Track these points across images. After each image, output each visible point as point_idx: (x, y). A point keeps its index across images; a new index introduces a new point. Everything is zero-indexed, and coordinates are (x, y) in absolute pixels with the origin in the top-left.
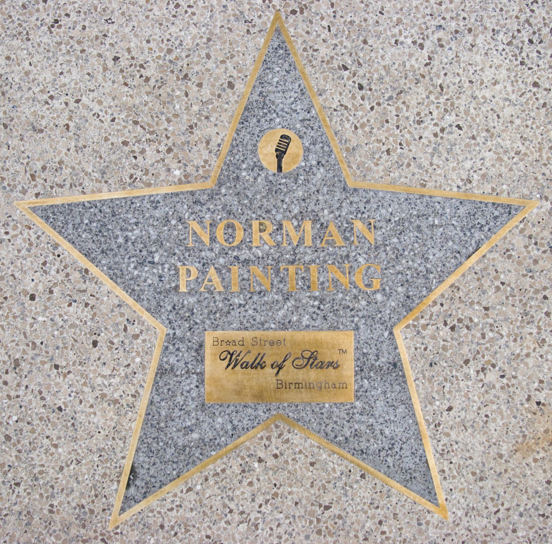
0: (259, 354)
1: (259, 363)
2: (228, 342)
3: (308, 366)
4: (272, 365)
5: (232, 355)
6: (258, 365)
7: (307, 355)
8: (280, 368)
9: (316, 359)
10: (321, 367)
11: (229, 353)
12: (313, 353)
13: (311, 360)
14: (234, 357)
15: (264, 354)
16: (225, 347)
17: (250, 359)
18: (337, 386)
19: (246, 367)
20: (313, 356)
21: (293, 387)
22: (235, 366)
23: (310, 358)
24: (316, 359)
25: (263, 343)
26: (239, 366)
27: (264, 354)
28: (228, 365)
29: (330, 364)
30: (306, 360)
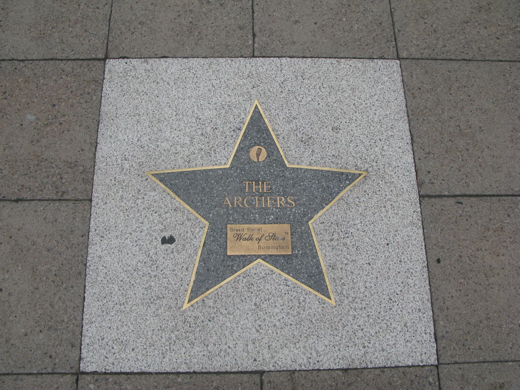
0: (250, 235)
1: (250, 239)
2: (237, 230)
4: (256, 239)
6: (250, 239)
7: (271, 235)
8: (260, 240)
11: (237, 234)
12: (273, 234)
15: (253, 235)
17: (246, 236)
18: (285, 248)
19: (245, 240)
20: (274, 235)
22: (240, 240)
23: (273, 236)
24: (275, 236)
25: (252, 230)
26: (242, 240)
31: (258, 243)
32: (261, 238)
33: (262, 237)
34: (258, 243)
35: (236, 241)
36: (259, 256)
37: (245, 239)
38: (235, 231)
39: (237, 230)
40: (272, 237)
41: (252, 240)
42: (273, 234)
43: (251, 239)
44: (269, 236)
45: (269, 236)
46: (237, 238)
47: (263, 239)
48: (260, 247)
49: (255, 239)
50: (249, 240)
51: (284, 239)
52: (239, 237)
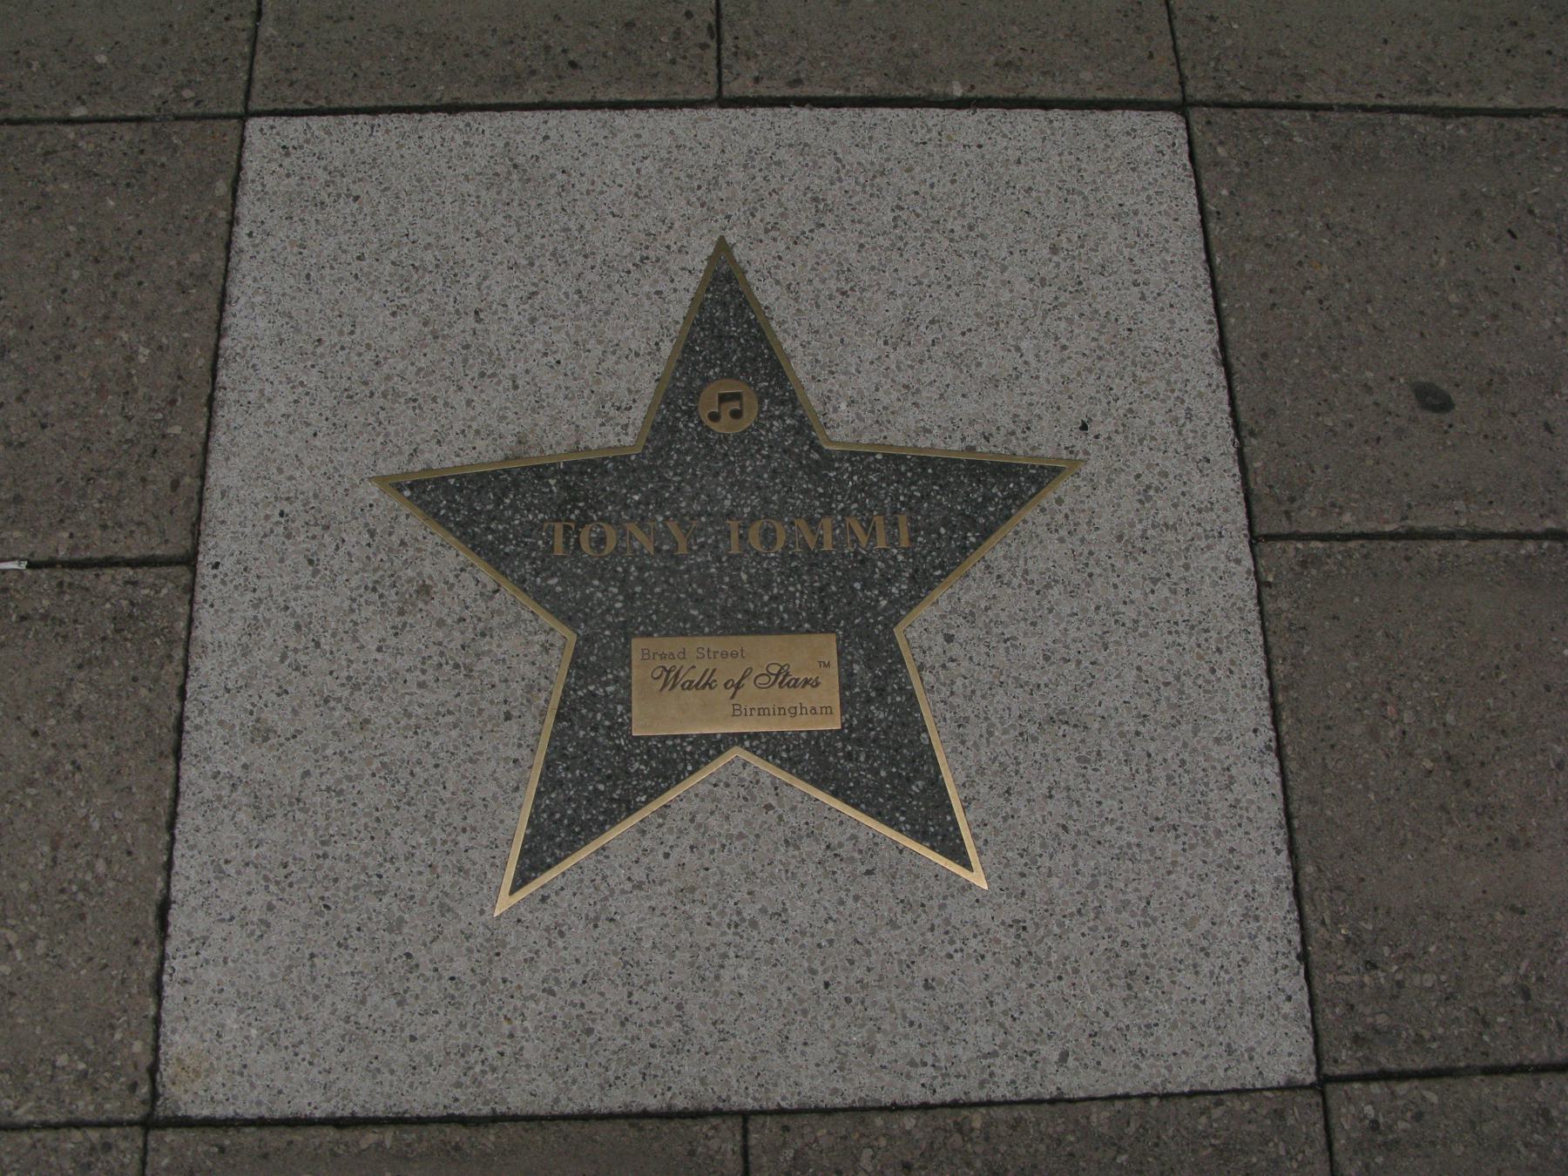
1: (706, 684)
2: (663, 656)
3: (777, 685)
4: (726, 685)
5: (669, 672)
7: (774, 670)
8: (738, 687)
9: (787, 675)
10: (794, 686)
11: (665, 668)
12: (782, 668)
13: (781, 678)
14: (673, 674)
15: (714, 671)
16: (659, 662)
18: (819, 711)
19: (688, 688)
21: (755, 713)
22: (674, 686)
23: (779, 673)
25: (711, 655)
26: (679, 686)
27: (714, 671)
28: (665, 685)
29: (807, 682)
30: (773, 678)
31: (732, 697)
32: (739, 682)
33: (743, 678)
34: (732, 697)
35: (662, 689)
36: (739, 739)
37: (690, 686)
38: (657, 657)
39: (663, 656)
40: (777, 676)
41: (711, 688)
42: (782, 668)
43: (709, 685)
44: (769, 674)
45: (769, 674)
46: (662, 681)
47: (749, 683)
48: (737, 712)
49: (721, 682)
50: (704, 687)
51: (818, 684)
52: (671, 679)
